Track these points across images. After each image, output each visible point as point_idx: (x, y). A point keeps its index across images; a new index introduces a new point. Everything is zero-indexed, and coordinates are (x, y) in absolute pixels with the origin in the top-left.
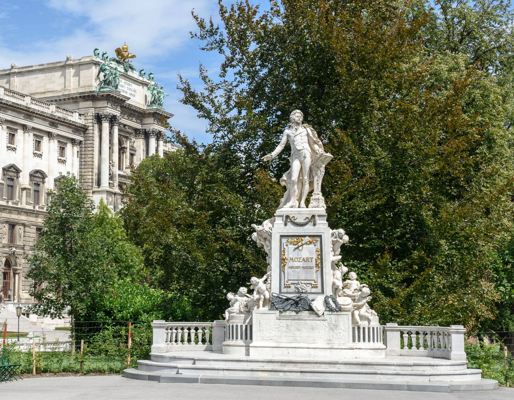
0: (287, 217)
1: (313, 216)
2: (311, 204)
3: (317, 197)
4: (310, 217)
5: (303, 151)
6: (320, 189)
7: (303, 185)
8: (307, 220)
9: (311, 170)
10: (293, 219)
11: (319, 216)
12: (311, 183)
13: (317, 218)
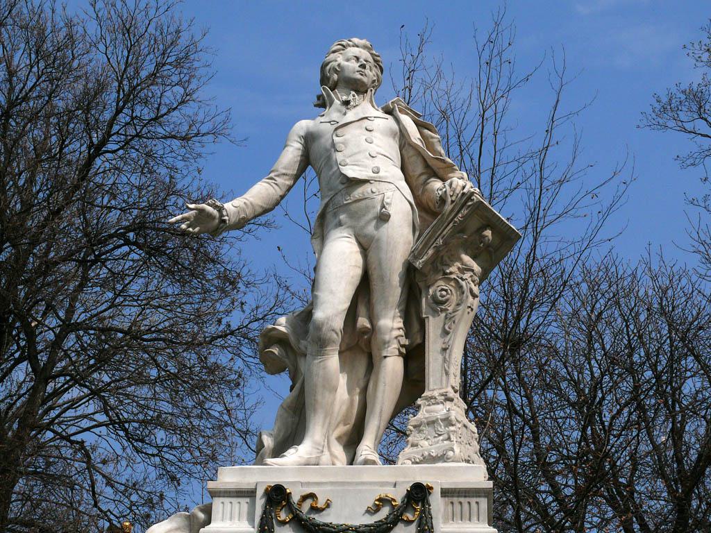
0: (277, 495)
1: (419, 493)
2: (408, 450)
3: (440, 410)
4: (398, 495)
5: (367, 188)
6: (456, 381)
7: (372, 366)
8: (385, 512)
9: (414, 281)
10: (306, 506)
11: (446, 493)
12: (414, 357)
13: (437, 503)
